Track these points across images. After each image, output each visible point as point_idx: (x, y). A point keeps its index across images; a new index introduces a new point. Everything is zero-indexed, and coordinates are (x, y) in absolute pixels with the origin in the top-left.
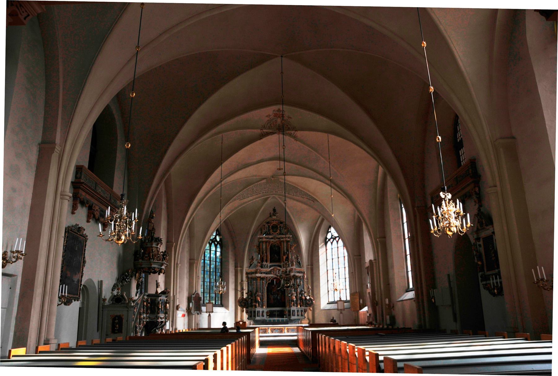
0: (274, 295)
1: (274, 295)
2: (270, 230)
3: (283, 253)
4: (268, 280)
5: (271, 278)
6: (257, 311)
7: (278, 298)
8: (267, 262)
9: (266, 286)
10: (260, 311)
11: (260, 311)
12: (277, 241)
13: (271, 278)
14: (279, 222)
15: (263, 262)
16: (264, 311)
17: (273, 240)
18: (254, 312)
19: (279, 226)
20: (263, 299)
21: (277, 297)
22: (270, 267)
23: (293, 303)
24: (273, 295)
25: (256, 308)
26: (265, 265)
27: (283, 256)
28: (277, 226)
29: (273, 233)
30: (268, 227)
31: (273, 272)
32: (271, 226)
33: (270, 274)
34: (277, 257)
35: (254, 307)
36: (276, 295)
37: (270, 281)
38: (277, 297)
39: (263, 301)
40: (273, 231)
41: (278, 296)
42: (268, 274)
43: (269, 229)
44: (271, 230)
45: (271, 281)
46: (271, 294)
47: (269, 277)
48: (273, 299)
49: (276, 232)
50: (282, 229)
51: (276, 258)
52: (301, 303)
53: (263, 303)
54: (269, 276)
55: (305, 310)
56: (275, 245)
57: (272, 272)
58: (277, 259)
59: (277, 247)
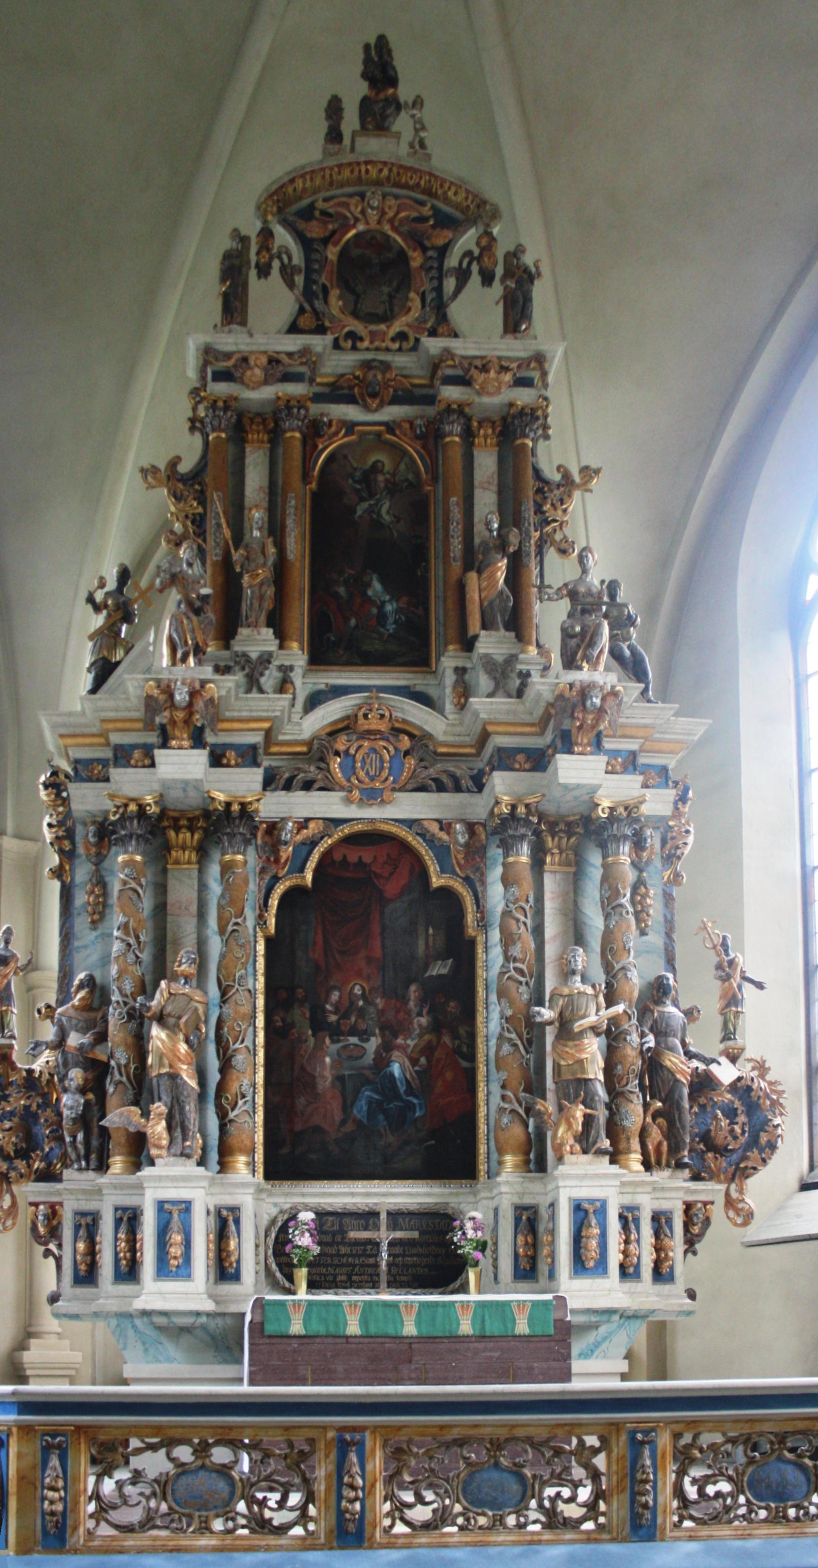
0: (353, 1040)
1: (353, 1032)
2: (325, 291)
3: (457, 546)
4: (286, 852)
5: (313, 843)
6: (161, 1205)
7: (396, 1069)
8: (282, 637)
9: (261, 919)
10: (186, 1207)
11: (186, 1207)
12: (390, 427)
13: (313, 843)
14: (426, 211)
15: (243, 632)
16: (235, 1210)
17: (352, 412)
18: (118, 1222)
19: (416, 259)
20: (226, 1066)
21: (382, 1061)
22: (314, 701)
23: (579, 1112)
24: (336, 1033)
25: (147, 1171)
26: (266, 660)
27: (457, 567)
28: (403, 257)
29: (359, 327)
30: (298, 258)
31: (350, 770)
32: (332, 253)
33: (307, 786)
34: (389, 608)
35: (117, 1163)
36: (364, 1036)
37: (309, 876)
38: (382, 1061)
39: (234, 1087)
40: (355, 314)
41: (387, 1047)
42: (288, 786)
43: (309, 281)
44: (334, 293)
45: (318, 872)
46: (318, 1025)
47: (303, 824)
48: (340, 1079)
49: (387, 318)
50: (459, 289)
51: (382, 617)
52: (655, 1135)
53: (222, 1115)
54: (302, 813)
55: (688, 1207)
56: (376, 468)
57: (336, 764)
58: (391, 628)
59: (393, 489)
